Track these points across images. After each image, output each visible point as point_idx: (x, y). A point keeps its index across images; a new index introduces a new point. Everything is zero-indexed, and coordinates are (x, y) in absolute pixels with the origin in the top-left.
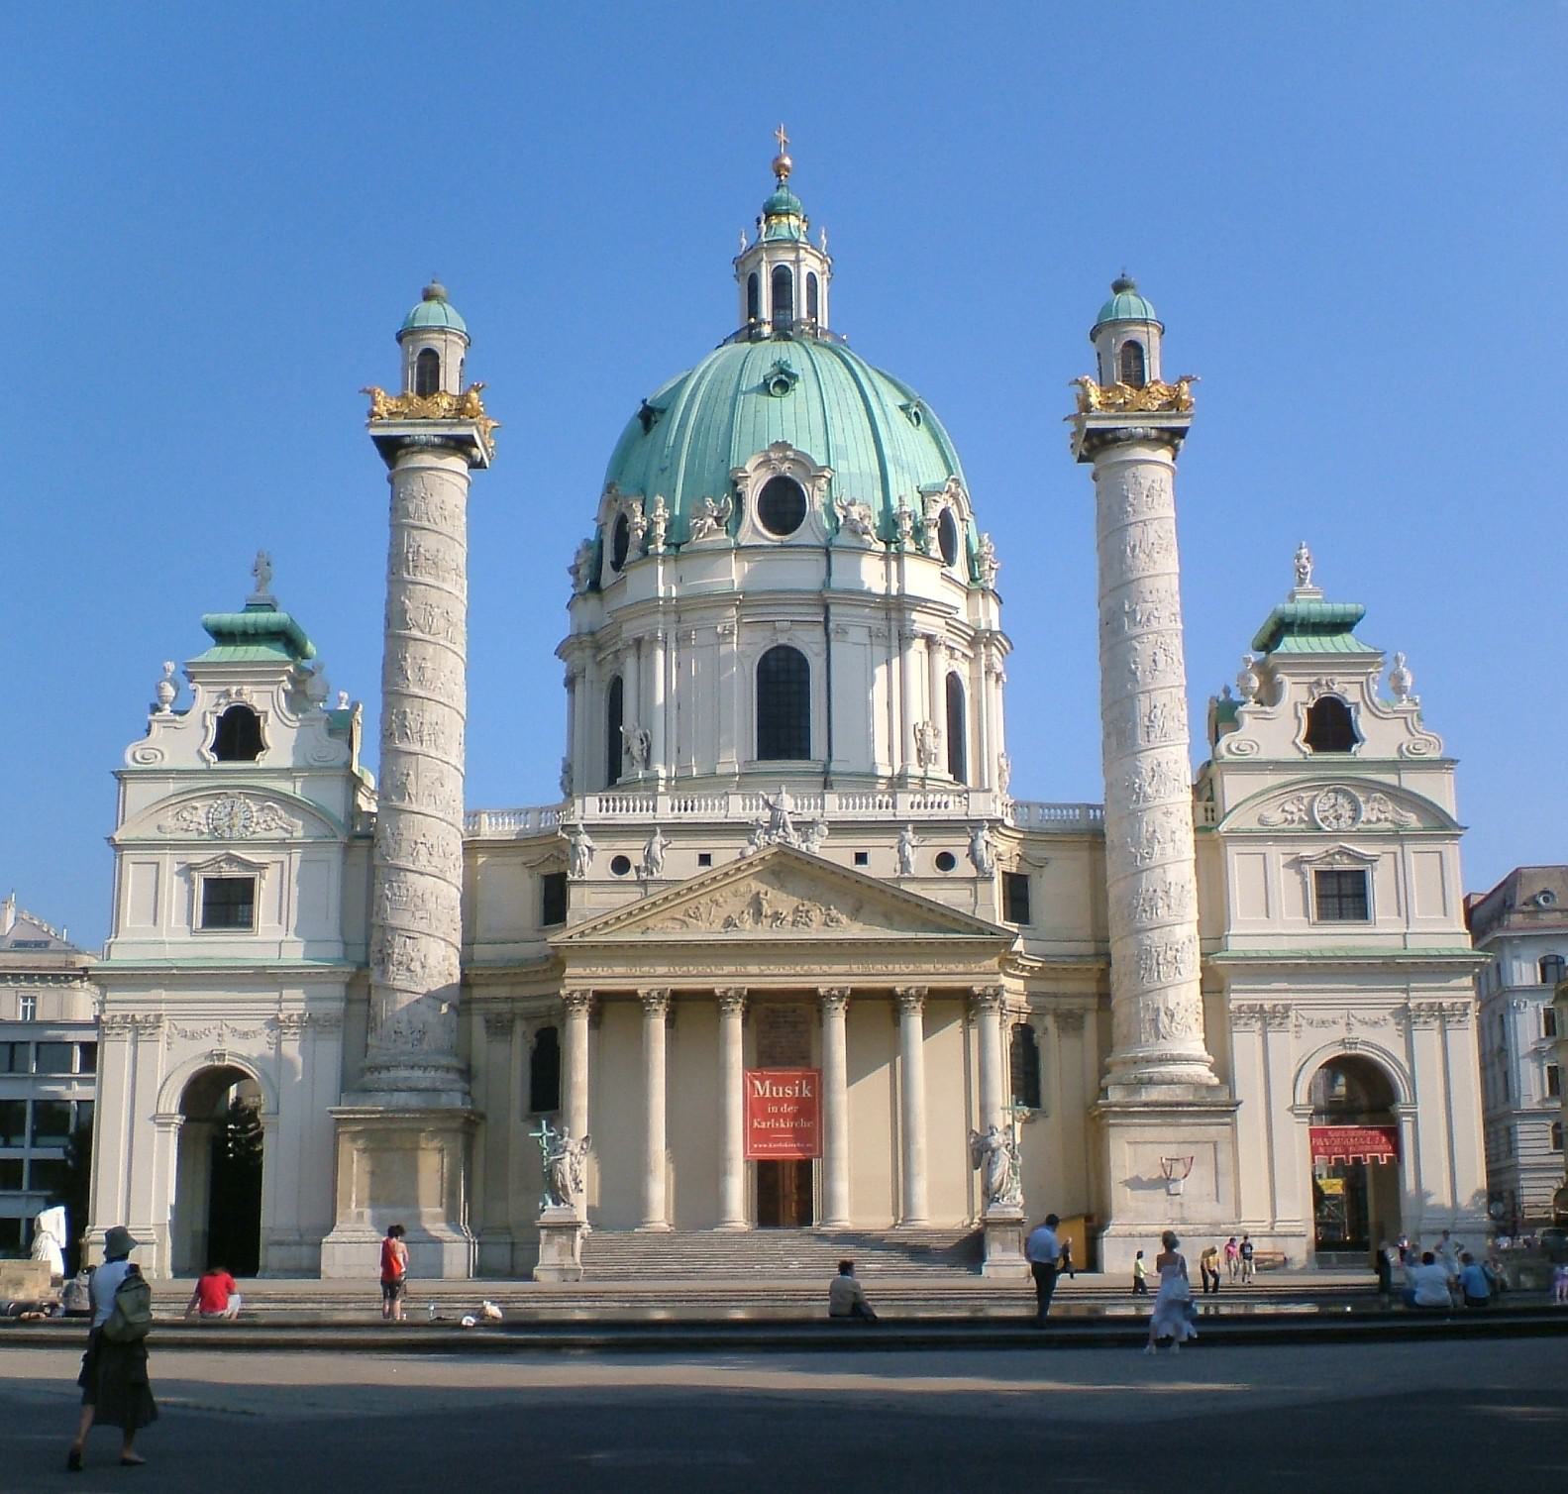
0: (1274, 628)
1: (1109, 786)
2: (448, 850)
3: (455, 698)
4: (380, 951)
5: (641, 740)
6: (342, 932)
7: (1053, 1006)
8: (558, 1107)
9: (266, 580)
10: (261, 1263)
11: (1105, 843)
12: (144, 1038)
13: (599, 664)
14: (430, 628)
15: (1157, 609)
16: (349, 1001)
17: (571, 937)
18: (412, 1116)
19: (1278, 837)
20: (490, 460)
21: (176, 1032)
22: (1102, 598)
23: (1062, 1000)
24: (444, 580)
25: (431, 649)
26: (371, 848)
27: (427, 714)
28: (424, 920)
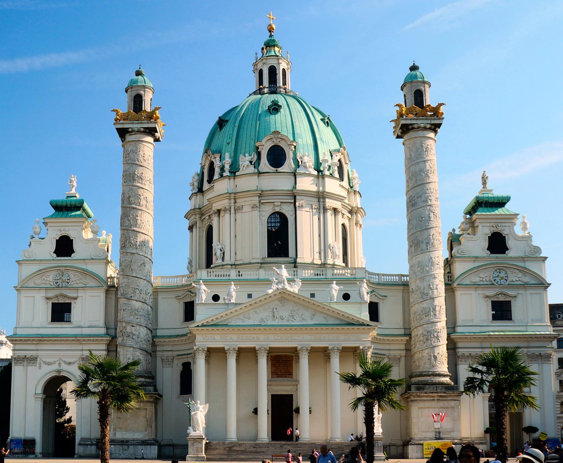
0: (474, 204)
1: (411, 267)
2: (149, 291)
4: (121, 331)
5: (221, 251)
6: (105, 325)
7: (388, 355)
8: (191, 393)
9: (73, 186)
10: (76, 453)
11: (409, 290)
12: (30, 364)
13: (202, 221)
14: (140, 203)
15: (430, 196)
16: (108, 351)
17: (198, 326)
19: (476, 286)
20: (162, 138)
21: (41, 362)
22: (408, 192)
23: (391, 352)
24: (145, 185)
25: (140, 212)
26: (117, 291)
27: (139, 237)
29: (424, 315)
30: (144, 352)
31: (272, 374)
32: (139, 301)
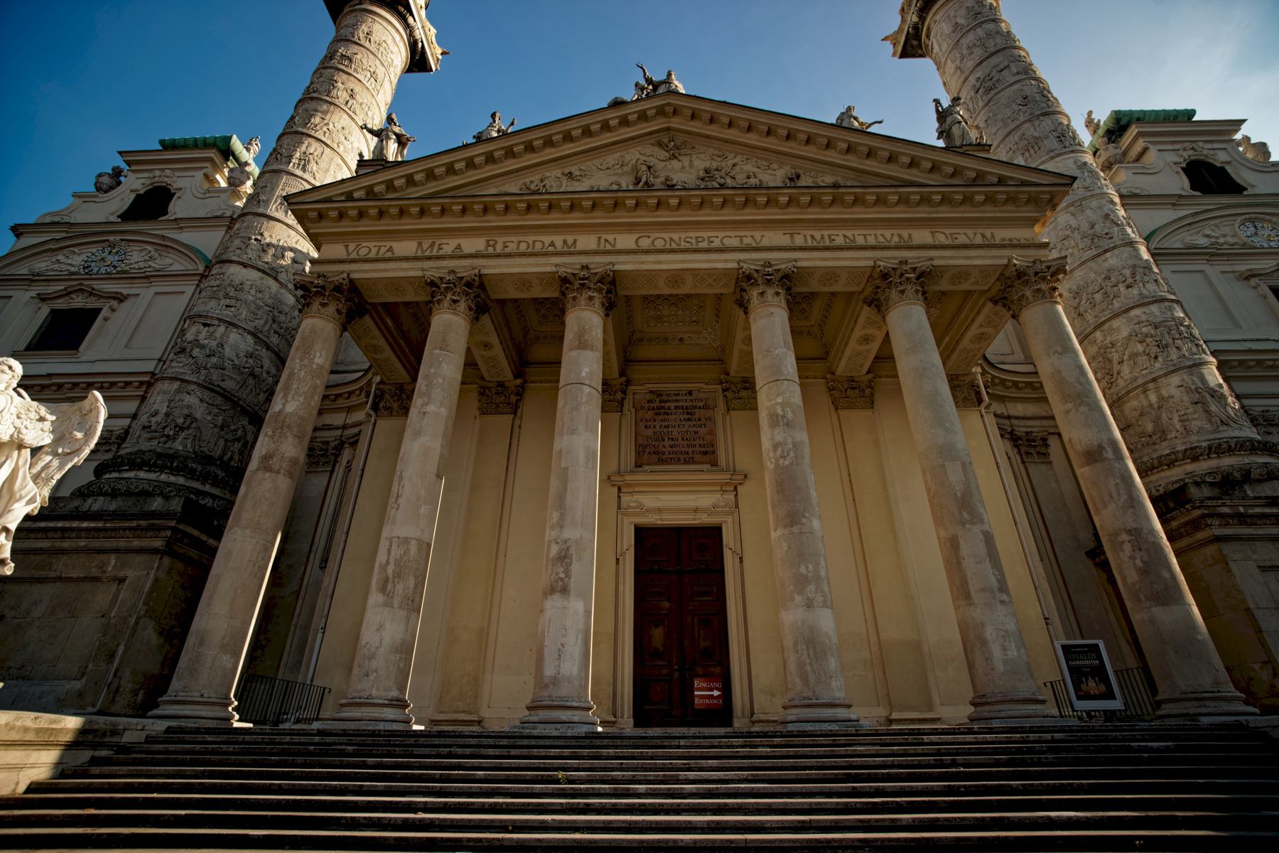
3: (342, 148)
14: (330, 92)
18: (92, 525)
23: (1014, 421)
24: (355, 70)
28: (233, 309)
29: (1122, 287)
30: (219, 398)
31: (639, 454)
32: (253, 267)
